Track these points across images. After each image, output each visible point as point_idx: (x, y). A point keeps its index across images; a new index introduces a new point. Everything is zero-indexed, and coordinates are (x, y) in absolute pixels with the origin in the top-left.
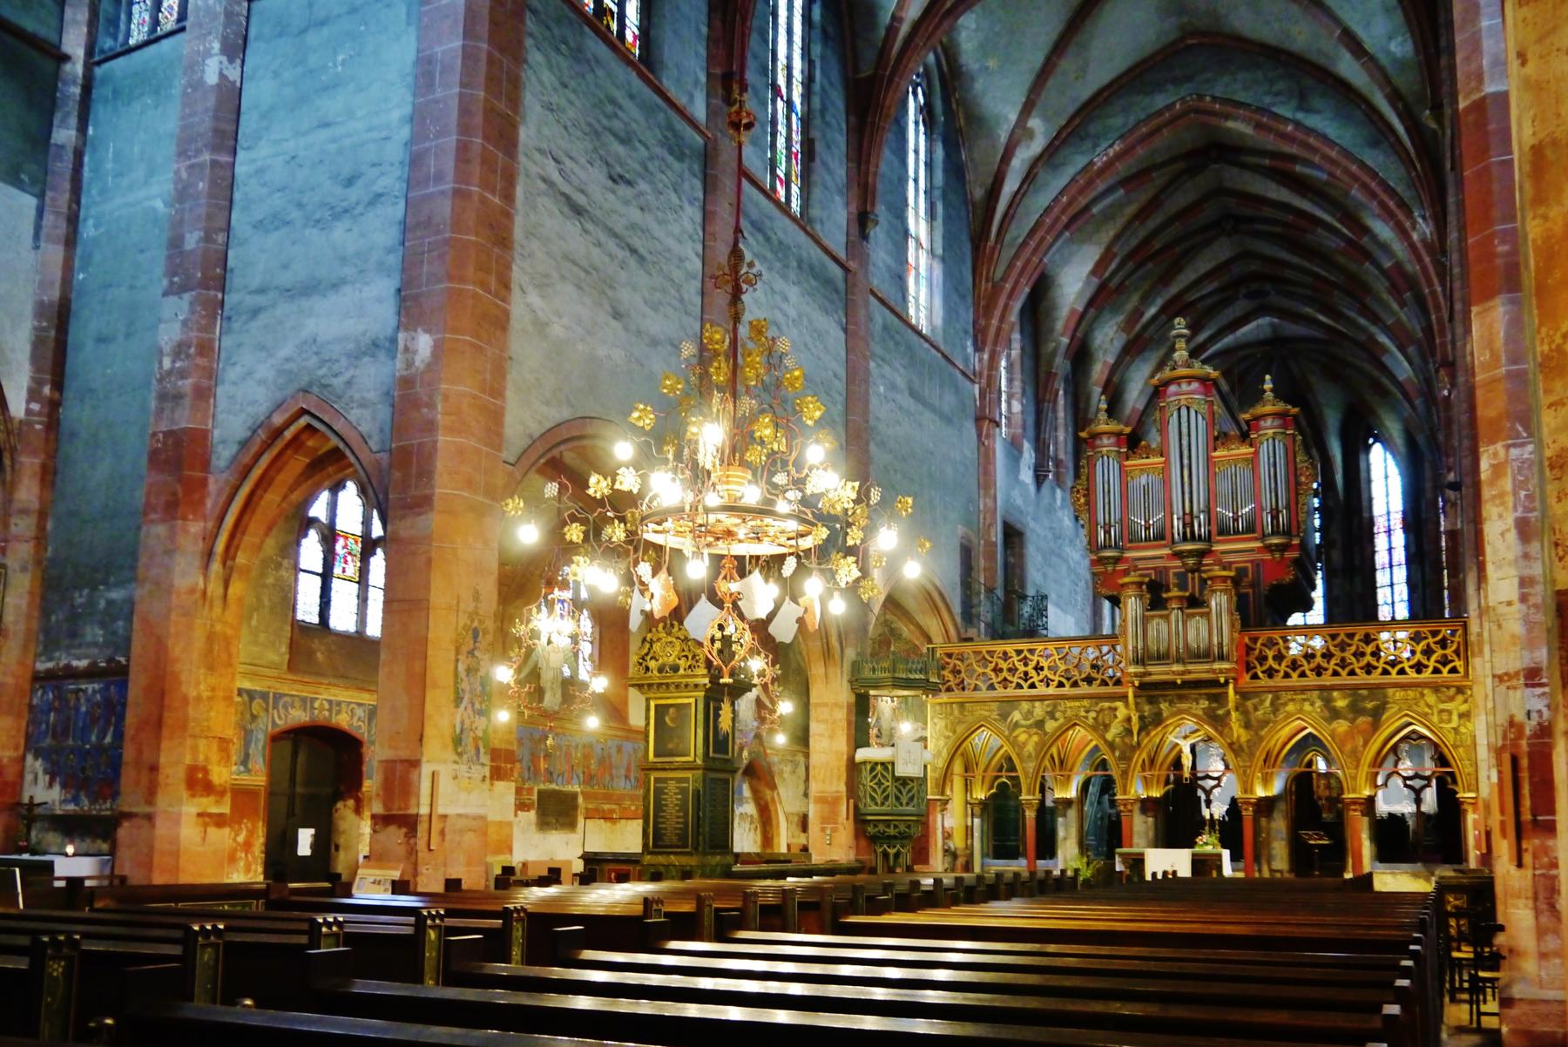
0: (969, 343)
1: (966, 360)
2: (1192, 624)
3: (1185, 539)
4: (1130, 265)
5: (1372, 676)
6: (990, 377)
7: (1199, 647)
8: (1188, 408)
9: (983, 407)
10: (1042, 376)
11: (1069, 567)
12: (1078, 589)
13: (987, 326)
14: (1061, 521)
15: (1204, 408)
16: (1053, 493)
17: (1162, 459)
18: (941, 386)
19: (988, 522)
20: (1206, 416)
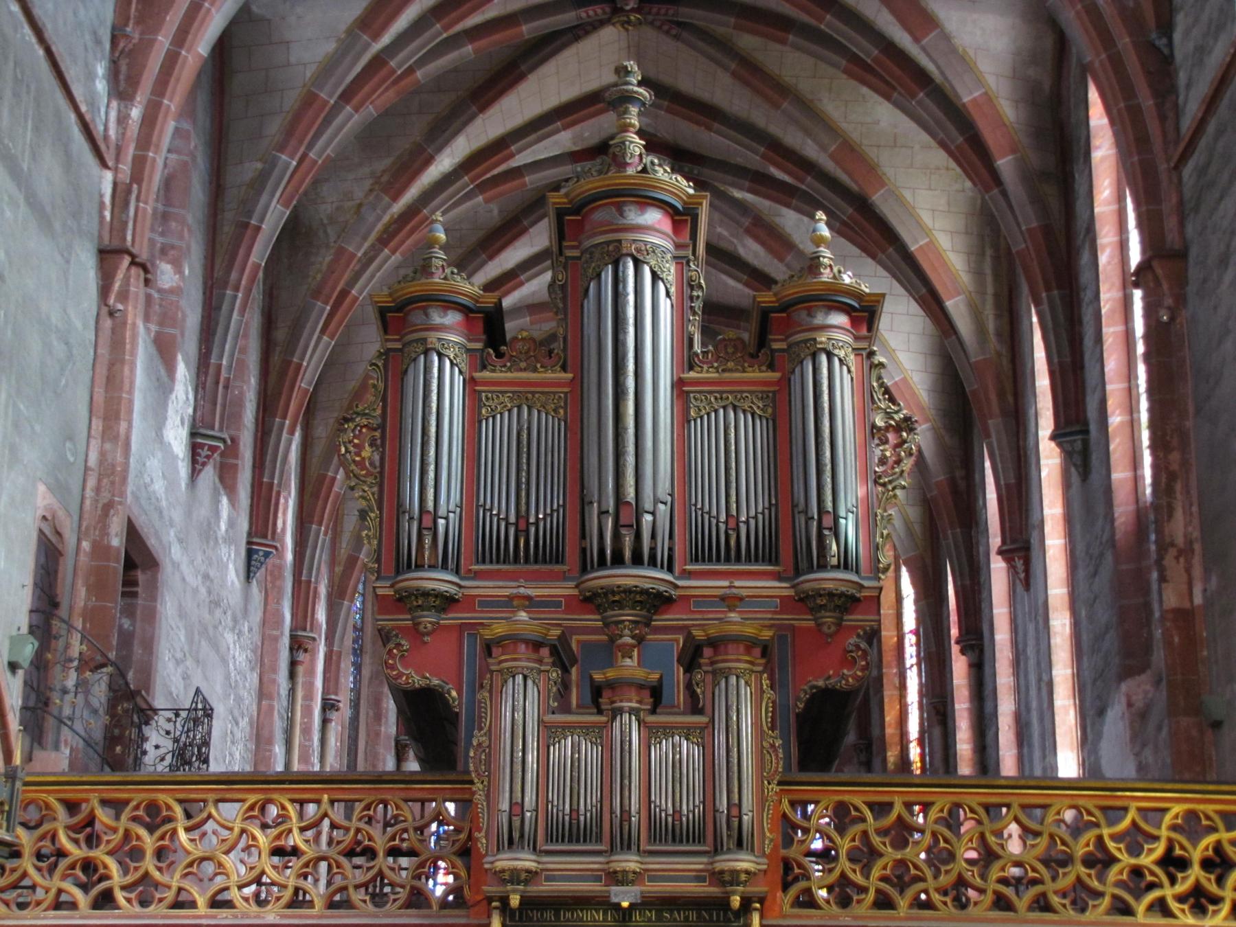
0: (101, 69)
1: (92, 104)
2: (662, 750)
3: (618, 560)
4: (438, 32)
5: (1089, 916)
6: (139, 163)
7: (677, 812)
8: (638, 264)
9: (118, 226)
10: (227, 229)
11: (228, 677)
12: (238, 735)
13: (146, 46)
14: (223, 568)
15: (670, 271)
16: (217, 502)
17: (570, 375)
18: (36, 129)
19: (105, 496)
20: (673, 290)
